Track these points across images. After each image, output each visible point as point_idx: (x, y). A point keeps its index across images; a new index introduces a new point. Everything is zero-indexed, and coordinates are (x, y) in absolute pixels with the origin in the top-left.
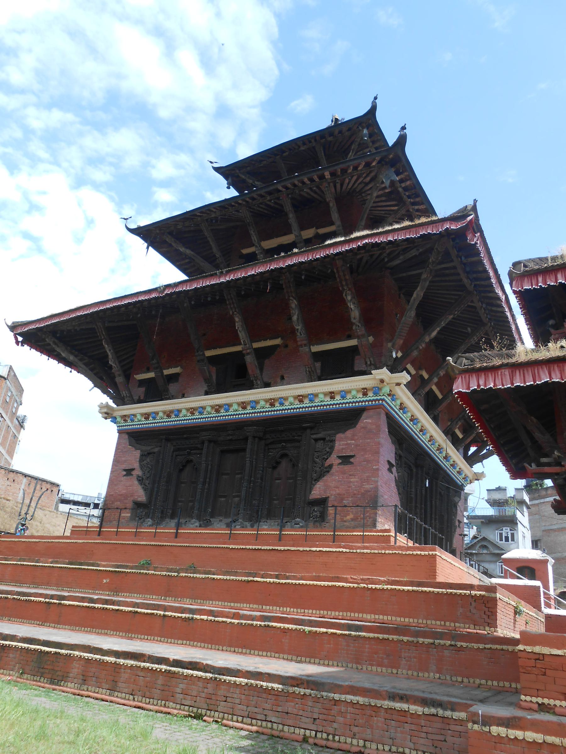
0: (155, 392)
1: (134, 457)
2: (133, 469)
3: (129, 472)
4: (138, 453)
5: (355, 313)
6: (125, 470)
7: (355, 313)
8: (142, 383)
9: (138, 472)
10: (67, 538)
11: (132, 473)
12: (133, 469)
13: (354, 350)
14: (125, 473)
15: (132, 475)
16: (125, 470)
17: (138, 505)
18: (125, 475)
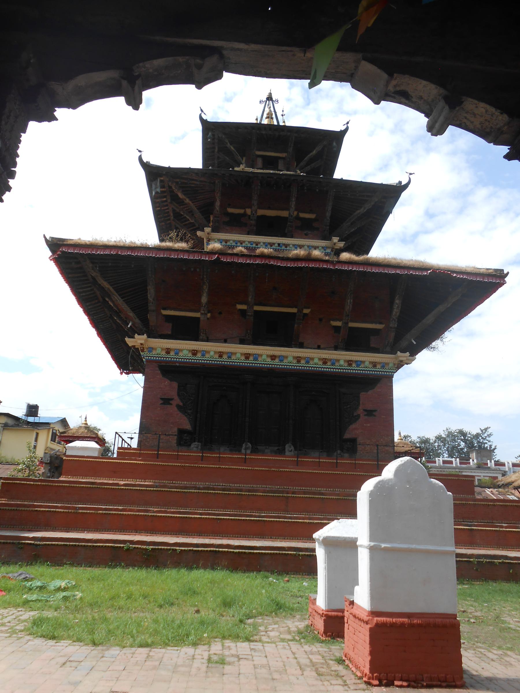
0: (186, 330)
1: (170, 388)
2: (172, 399)
3: (166, 401)
4: (175, 385)
5: (396, 311)
6: (162, 399)
7: (396, 311)
8: (168, 318)
9: (177, 401)
10: (115, 459)
11: (171, 402)
12: (172, 399)
13: (376, 332)
14: (162, 402)
15: (171, 404)
16: (162, 399)
17: (181, 432)
18: (161, 404)
